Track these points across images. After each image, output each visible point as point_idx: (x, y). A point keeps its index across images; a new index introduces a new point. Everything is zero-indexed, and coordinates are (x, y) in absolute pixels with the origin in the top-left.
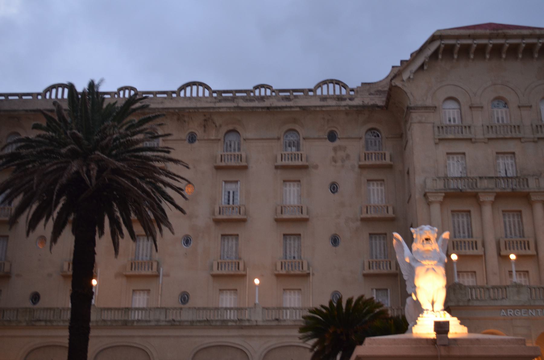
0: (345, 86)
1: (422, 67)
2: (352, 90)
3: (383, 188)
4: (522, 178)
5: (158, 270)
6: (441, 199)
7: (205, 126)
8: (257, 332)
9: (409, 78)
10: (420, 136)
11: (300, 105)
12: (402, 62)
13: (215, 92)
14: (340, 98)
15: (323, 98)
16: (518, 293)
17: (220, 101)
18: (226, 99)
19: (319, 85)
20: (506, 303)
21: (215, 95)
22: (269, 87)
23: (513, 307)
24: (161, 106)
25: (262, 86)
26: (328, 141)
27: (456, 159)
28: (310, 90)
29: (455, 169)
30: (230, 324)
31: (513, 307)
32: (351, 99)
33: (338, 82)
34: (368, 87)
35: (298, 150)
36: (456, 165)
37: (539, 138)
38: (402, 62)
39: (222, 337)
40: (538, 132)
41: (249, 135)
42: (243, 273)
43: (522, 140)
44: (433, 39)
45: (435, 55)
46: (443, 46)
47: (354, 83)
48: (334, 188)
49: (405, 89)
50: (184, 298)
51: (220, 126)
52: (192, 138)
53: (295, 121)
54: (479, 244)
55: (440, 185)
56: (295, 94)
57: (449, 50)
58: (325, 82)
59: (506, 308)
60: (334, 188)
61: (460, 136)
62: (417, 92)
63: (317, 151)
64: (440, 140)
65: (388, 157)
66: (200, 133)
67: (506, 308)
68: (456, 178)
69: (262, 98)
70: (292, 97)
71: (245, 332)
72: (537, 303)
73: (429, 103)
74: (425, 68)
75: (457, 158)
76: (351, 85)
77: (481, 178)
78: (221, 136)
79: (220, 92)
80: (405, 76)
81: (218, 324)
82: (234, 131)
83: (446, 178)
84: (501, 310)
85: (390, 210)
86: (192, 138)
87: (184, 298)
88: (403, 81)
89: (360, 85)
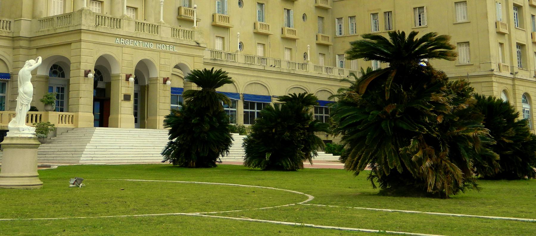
16: (129, 24)
23: (125, 37)
84: (117, 37)
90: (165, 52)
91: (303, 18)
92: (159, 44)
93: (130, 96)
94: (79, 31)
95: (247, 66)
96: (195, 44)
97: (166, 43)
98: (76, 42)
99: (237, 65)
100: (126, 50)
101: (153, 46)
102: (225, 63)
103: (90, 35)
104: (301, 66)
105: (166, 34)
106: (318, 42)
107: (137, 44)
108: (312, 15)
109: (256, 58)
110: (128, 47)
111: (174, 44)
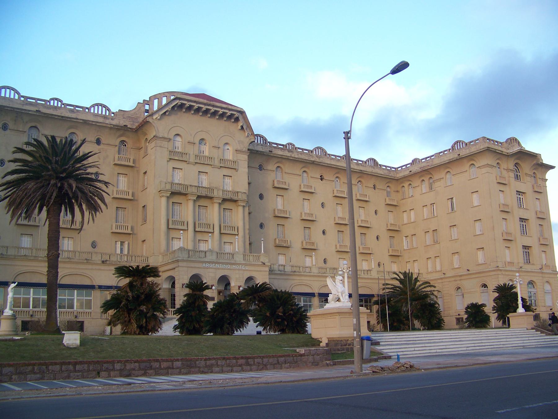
0: (109, 110)
1: (165, 113)
2: (113, 113)
3: (126, 179)
4: (211, 189)
7: (15, 121)
12: (144, 100)
13: (23, 97)
14: (105, 117)
15: (97, 115)
17: (27, 104)
18: (31, 104)
19: (93, 106)
20: (206, 260)
21: (22, 99)
22: (61, 101)
23: (209, 262)
25: (56, 99)
28: (87, 108)
30: (40, 259)
31: (209, 262)
32: (112, 119)
33: (105, 106)
34: (122, 113)
38: (144, 100)
39: (34, 266)
42: (38, 224)
45: (173, 108)
47: (114, 110)
51: (27, 122)
54: (186, 223)
55: (168, 187)
56: (77, 109)
58: (98, 105)
59: (206, 262)
65: (132, 161)
67: (206, 262)
68: (178, 184)
69: (56, 108)
70: (75, 111)
72: (220, 261)
73: (166, 136)
74: (167, 114)
76: (113, 111)
77: (190, 185)
78: (26, 129)
79: (27, 98)
80: (155, 117)
81: (32, 258)
82: (35, 127)
83: (172, 184)
85: (130, 193)
86: (5, 127)
90: (239, 270)
91: (377, 238)
93: (214, 298)
94: (178, 261)
95: (320, 274)
96: (261, 263)
97: (239, 264)
98: (177, 267)
99: (312, 274)
100: (211, 270)
102: (302, 274)
103: (185, 263)
104: (366, 272)
105: (239, 258)
106: (390, 254)
108: (385, 236)
109: (328, 269)
110: (211, 268)
111: (246, 265)
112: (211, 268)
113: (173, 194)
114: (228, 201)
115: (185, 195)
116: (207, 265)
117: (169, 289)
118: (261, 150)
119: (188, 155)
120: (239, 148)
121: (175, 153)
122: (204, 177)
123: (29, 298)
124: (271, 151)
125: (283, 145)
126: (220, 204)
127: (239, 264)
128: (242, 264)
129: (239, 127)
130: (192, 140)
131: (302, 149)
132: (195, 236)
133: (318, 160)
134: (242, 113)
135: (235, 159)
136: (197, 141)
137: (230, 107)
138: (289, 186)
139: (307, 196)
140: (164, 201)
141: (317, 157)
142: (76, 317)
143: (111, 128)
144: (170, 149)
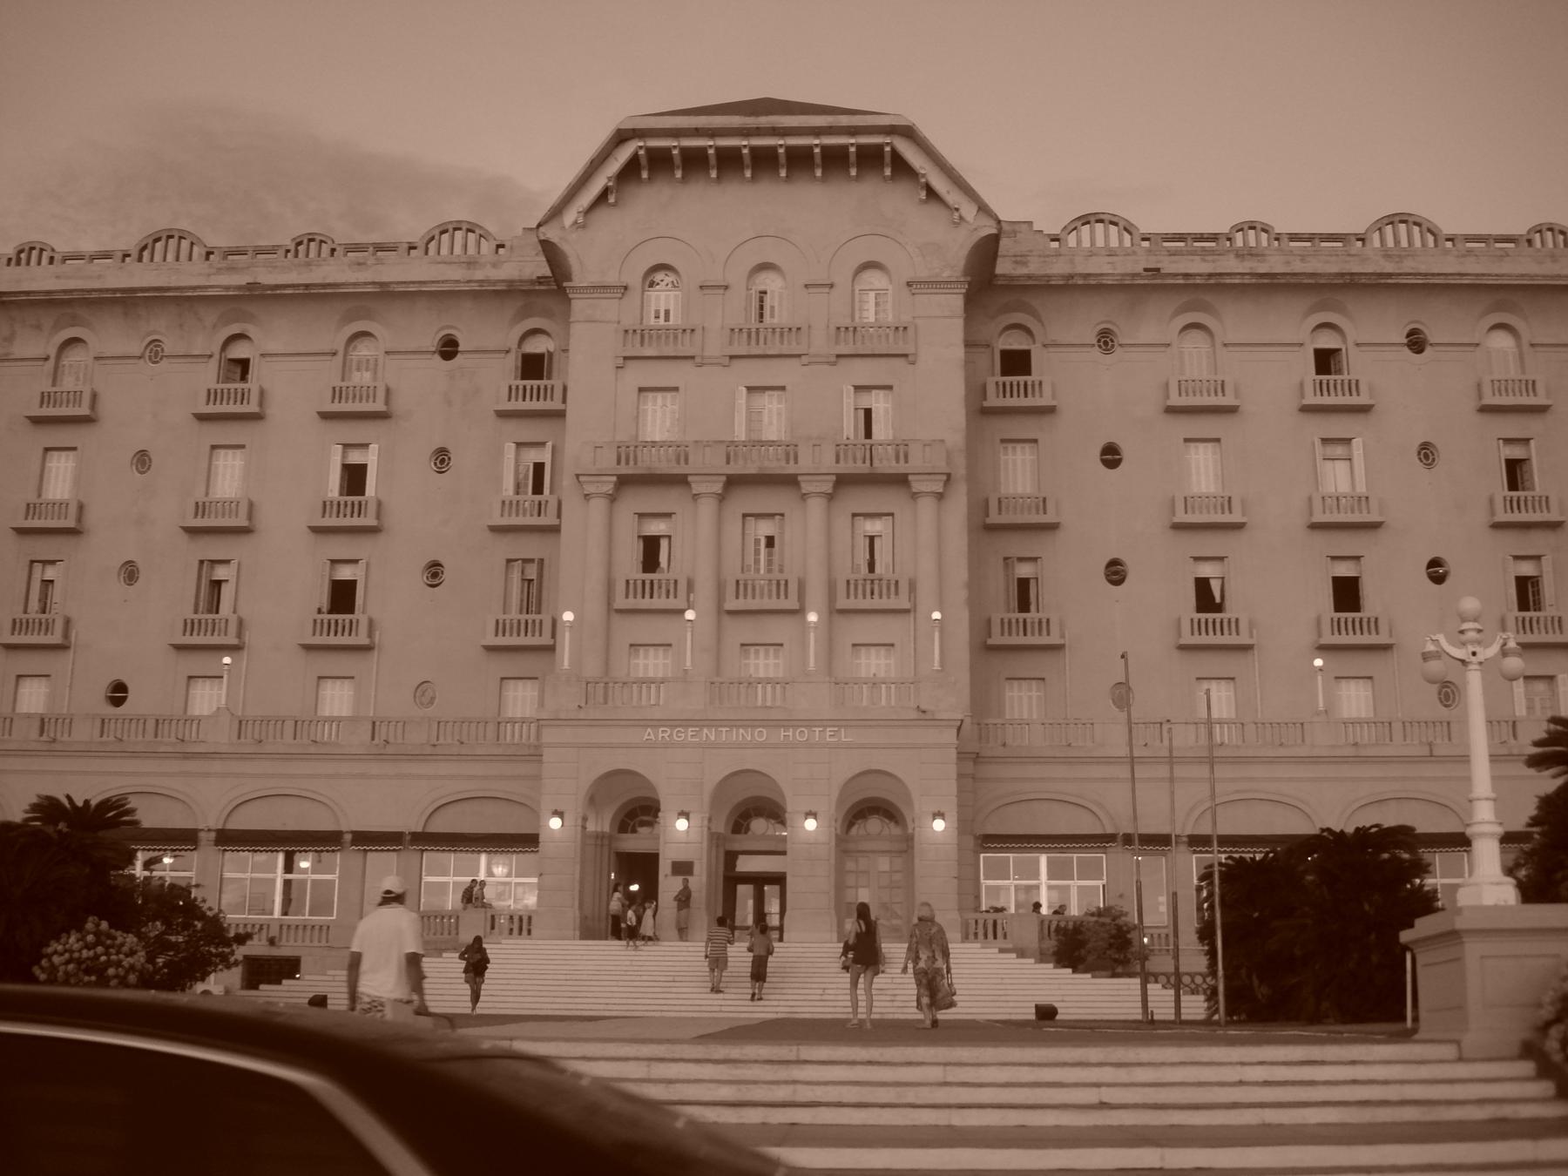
5: (66, 635)
6: (608, 488)
8: (217, 766)
9: (576, 222)
10: (587, 350)
11: (385, 279)
23: (672, 723)
24: (97, 285)
26: (437, 357)
27: (659, 401)
29: (659, 422)
31: (672, 723)
35: (375, 378)
36: (659, 414)
37: (838, 356)
40: (837, 343)
41: (272, 347)
43: (805, 360)
44: (621, 137)
45: (630, 171)
46: (642, 152)
48: (442, 458)
49: (565, 247)
50: (118, 693)
52: (155, 351)
53: (368, 315)
57: (659, 162)
60: (442, 458)
61: (669, 351)
62: (595, 252)
63: (417, 381)
64: (625, 358)
66: (169, 346)
71: (191, 766)
73: (612, 278)
74: (612, 199)
75: (664, 398)
87: (118, 693)
88: (563, 228)
89: (520, 232)
92: (786, 728)
96: (914, 715)
97: (809, 723)
101: (761, 735)
107: (709, 734)
112: (683, 746)
113: (624, 482)
114: (867, 480)
115: (681, 481)
116: (663, 734)
117: (611, 837)
118: (1107, 269)
119: (698, 332)
120: (923, 274)
121: (643, 335)
122: (771, 405)
123: (274, 881)
124: (1158, 270)
125: (1214, 237)
126: (830, 497)
127: (809, 723)
128: (823, 723)
129: (923, 195)
130: (716, 277)
131: (1310, 238)
132: (719, 628)
133: (1389, 267)
134: (908, 133)
135: (905, 319)
136: (736, 276)
137: (844, 120)
138: (1237, 397)
139: (1337, 426)
140: (598, 506)
141: (1387, 255)
142: (272, 942)
143: (476, 295)
144: (629, 321)
